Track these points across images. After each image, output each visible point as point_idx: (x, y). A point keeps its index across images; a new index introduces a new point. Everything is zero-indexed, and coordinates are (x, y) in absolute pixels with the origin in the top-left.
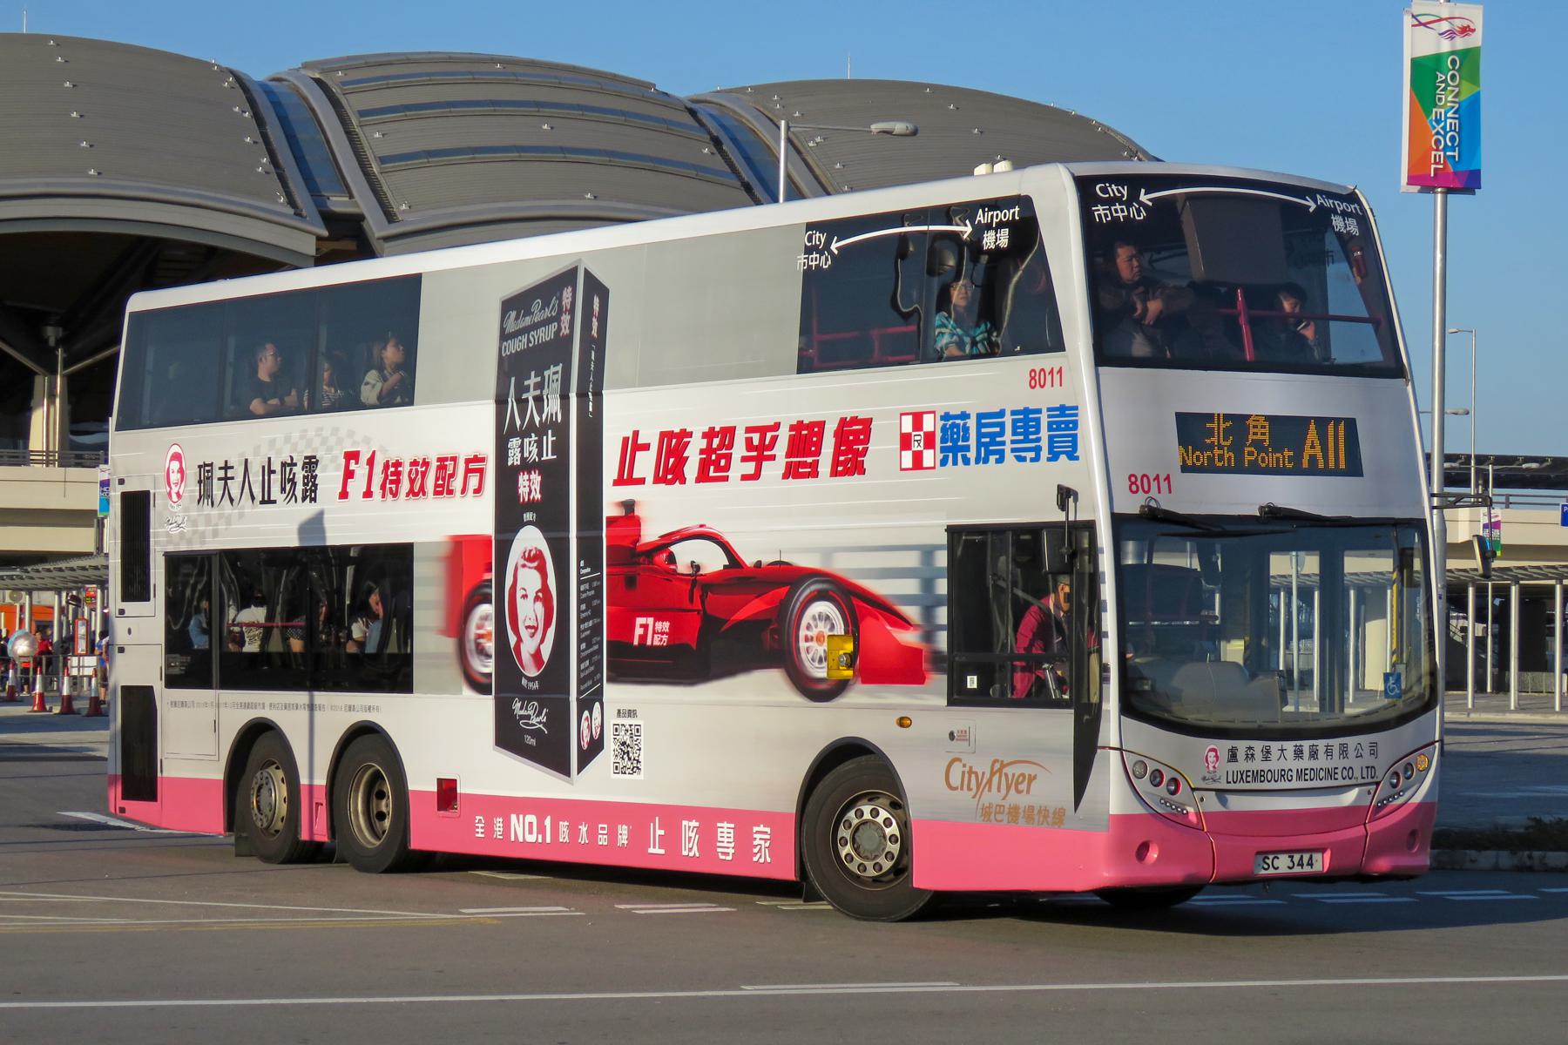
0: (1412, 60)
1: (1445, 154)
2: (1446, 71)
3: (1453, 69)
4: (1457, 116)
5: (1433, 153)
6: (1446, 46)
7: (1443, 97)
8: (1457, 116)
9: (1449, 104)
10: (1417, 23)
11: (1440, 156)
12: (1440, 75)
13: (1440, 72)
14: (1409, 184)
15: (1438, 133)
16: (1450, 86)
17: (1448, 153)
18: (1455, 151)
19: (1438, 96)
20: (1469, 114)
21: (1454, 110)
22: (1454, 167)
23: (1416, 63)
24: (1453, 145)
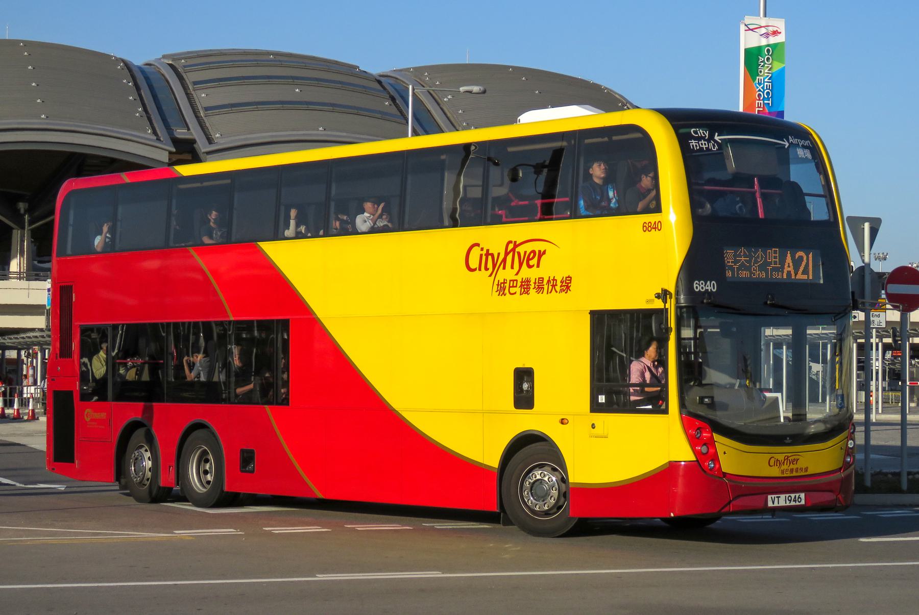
0: (745, 49)
1: (763, 103)
2: (764, 55)
3: (768, 55)
4: (770, 81)
5: (757, 102)
6: (764, 42)
7: (763, 70)
8: (770, 81)
9: (766, 74)
10: (748, 29)
11: (761, 103)
12: (760, 58)
13: (761, 56)
15: (760, 90)
16: (766, 64)
17: (765, 102)
18: (769, 101)
19: (759, 70)
20: (777, 81)
21: (768, 78)
23: (747, 51)
24: (768, 97)
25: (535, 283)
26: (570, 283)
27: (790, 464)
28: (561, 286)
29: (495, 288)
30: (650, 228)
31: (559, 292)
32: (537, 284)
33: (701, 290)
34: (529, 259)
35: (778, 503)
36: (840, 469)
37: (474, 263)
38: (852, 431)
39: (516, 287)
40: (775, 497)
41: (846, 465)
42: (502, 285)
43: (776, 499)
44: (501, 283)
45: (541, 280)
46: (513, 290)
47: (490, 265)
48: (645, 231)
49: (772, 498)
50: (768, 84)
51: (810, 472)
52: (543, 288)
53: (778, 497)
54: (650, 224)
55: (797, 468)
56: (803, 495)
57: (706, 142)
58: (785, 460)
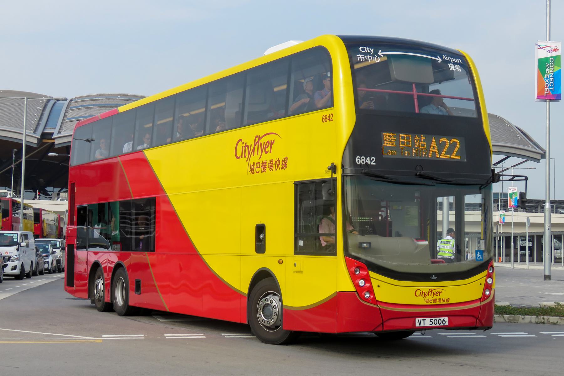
1: (549, 89)
3: (552, 62)
4: (553, 77)
6: (549, 55)
7: (548, 71)
8: (553, 77)
9: (550, 73)
11: (547, 89)
14: (537, 98)
15: (547, 82)
16: (550, 67)
17: (550, 89)
20: (557, 76)
21: (552, 75)
22: (552, 93)
25: (269, 164)
26: (287, 162)
27: (434, 295)
28: (282, 165)
29: (249, 168)
30: (326, 121)
31: (281, 168)
32: (270, 164)
33: (362, 163)
34: (266, 147)
35: (424, 325)
36: (480, 299)
37: (239, 154)
38: (491, 271)
39: (259, 167)
40: (421, 320)
41: (485, 297)
42: (253, 166)
43: (422, 321)
44: (252, 165)
45: (272, 162)
46: (258, 170)
47: (247, 154)
48: (323, 122)
49: (418, 320)
50: (552, 78)
51: (450, 302)
52: (273, 167)
53: (424, 320)
54: (326, 117)
55: (440, 299)
56: (446, 319)
57: (371, 56)
58: (429, 292)
